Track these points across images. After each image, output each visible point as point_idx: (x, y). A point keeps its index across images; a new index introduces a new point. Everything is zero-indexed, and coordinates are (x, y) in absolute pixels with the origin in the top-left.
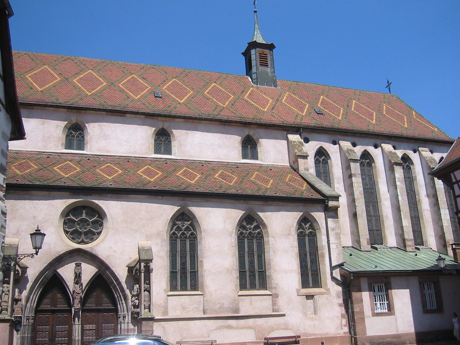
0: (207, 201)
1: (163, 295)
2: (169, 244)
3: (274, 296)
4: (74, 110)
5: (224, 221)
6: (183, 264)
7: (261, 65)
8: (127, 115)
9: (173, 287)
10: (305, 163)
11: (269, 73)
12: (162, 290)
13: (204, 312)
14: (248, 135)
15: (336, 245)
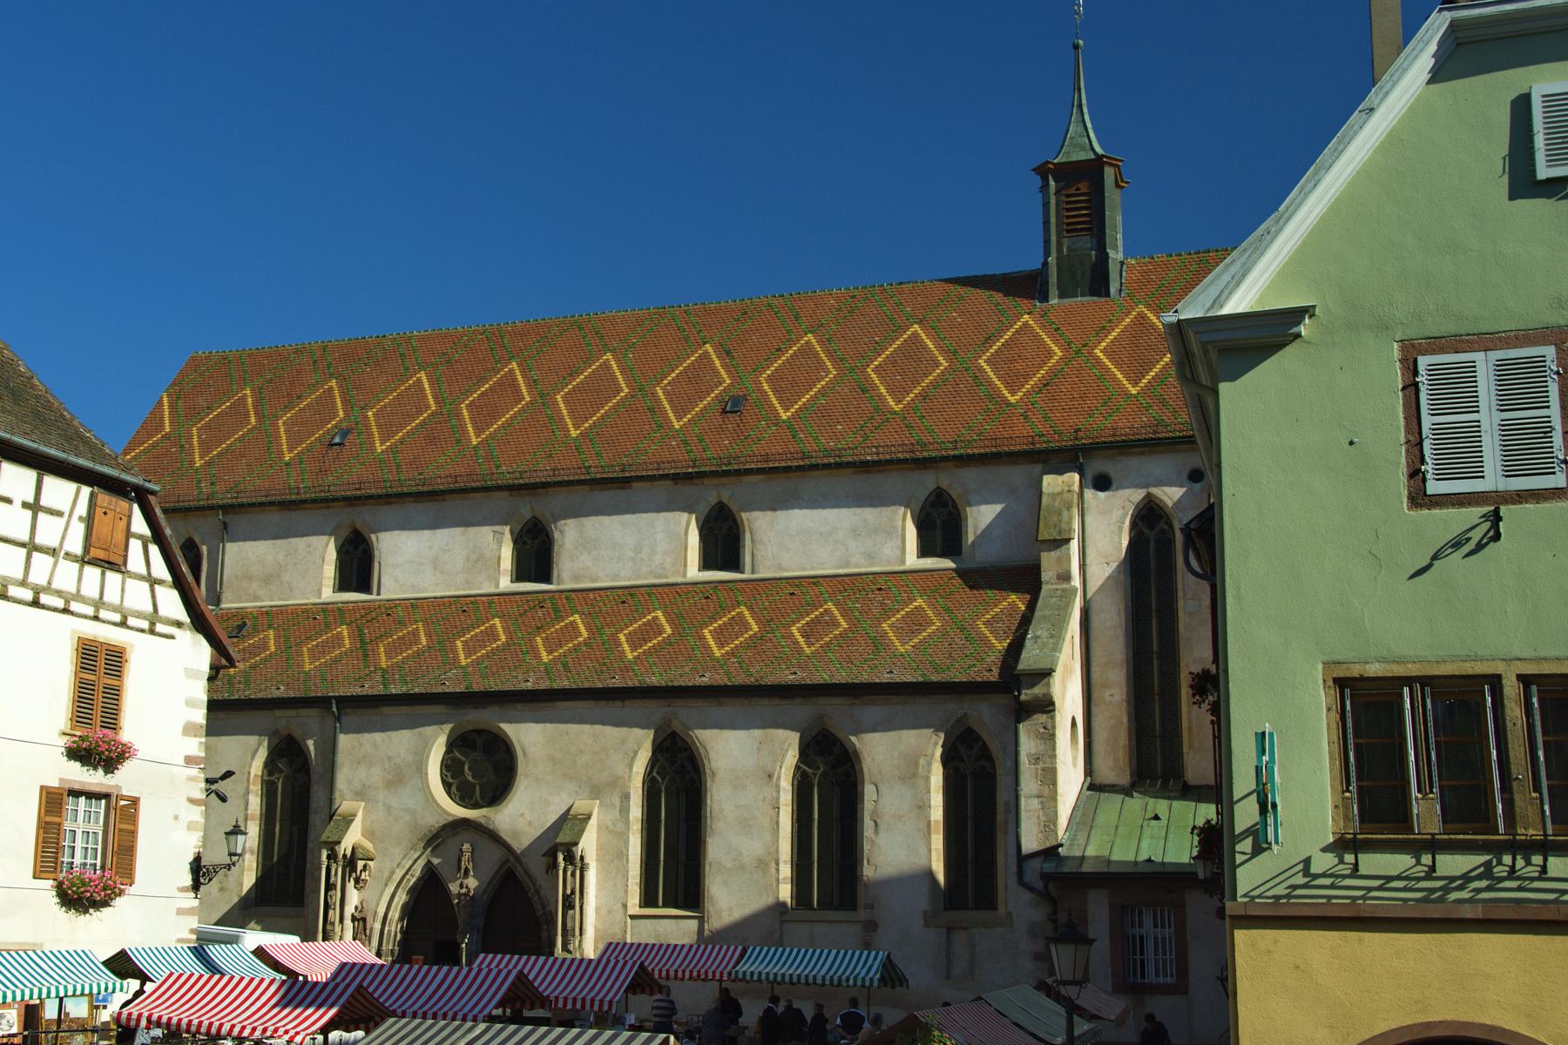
0: (720, 704)
2: (641, 803)
4: (523, 492)
5: (758, 749)
8: (635, 485)
9: (648, 899)
10: (1059, 560)
14: (939, 488)
15: (1041, 799)
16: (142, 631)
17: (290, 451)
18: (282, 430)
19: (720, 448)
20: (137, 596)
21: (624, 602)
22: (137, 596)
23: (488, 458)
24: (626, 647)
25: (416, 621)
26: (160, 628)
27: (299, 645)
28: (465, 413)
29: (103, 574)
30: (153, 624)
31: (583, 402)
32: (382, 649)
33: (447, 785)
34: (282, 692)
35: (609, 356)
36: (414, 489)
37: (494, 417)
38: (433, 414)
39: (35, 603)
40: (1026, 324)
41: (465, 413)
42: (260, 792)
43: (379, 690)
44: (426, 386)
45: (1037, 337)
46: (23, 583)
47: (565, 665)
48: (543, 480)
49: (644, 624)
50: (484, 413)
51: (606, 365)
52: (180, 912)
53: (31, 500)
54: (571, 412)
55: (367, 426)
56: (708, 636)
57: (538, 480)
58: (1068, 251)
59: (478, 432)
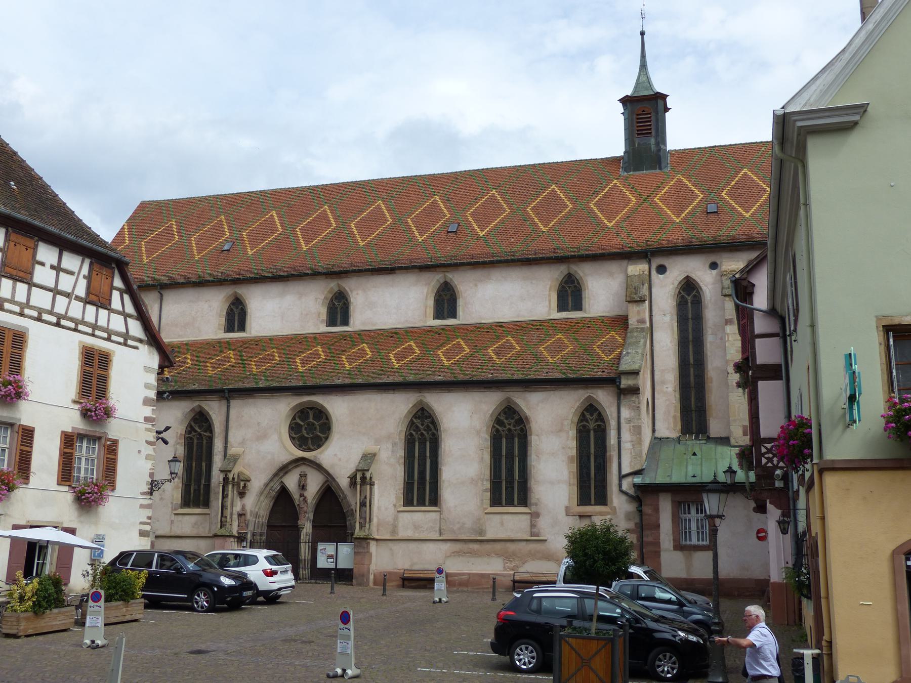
1: (392, 511)
2: (404, 448)
3: (535, 515)
5: (471, 416)
6: (422, 473)
7: (638, 134)
9: (408, 502)
10: (638, 312)
11: (652, 146)
12: (392, 505)
13: (440, 534)
15: (632, 443)
16: (119, 343)
17: (198, 255)
18: (194, 243)
19: (446, 251)
20: (117, 323)
21: (391, 337)
22: (117, 323)
23: (313, 258)
24: (394, 361)
25: (273, 348)
26: (130, 342)
27: (205, 361)
28: (299, 233)
29: (97, 310)
30: (126, 340)
31: (367, 226)
32: (253, 363)
33: (292, 438)
34: (196, 387)
35: (380, 202)
36: (270, 274)
37: (316, 235)
38: (280, 234)
39: (58, 325)
40: (615, 185)
41: (299, 233)
43: (252, 385)
44: (276, 219)
45: (621, 191)
46: (51, 313)
47: (360, 371)
48: (345, 269)
49: (404, 349)
50: (309, 234)
51: (379, 207)
52: (142, 506)
53: (55, 264)
54: (359, 232)
55: (243, 241)
56: (441, 355)
57: (342, 269)
58: (638, 145)
59: (307, 242)
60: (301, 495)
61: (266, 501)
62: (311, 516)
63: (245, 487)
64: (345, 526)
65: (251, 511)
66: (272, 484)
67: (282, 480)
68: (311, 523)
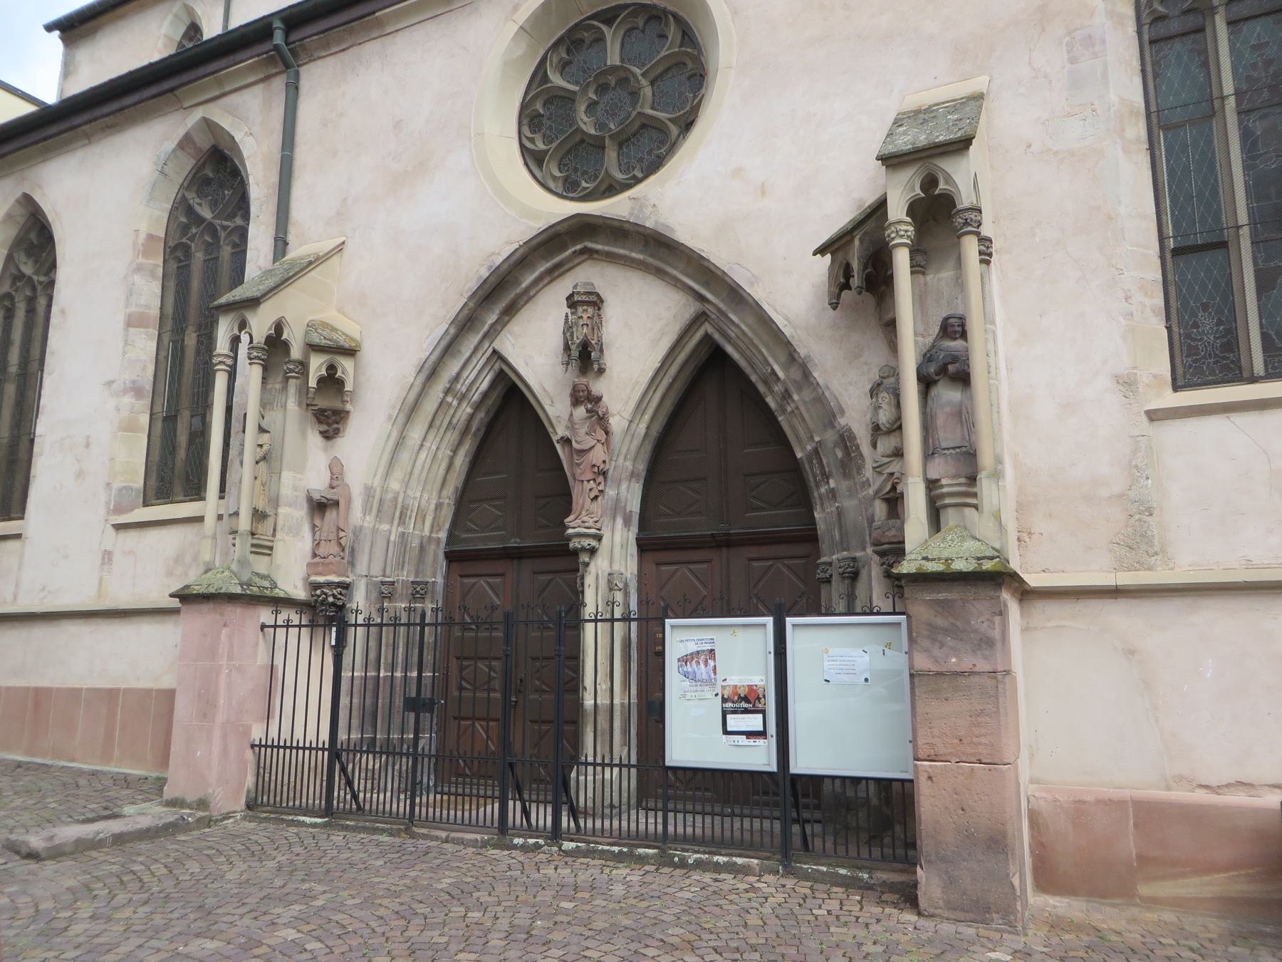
2: (1136, 64)
33: (533, 158)
42: (160, 271)
60: (581, 397)
61: (431, 444)
62: (632, 495)
63: (332, 382)
64: (810, 537)
65: (368, 492)
66: (453, 367)
67: (497, 345)
68: (634, 529)
